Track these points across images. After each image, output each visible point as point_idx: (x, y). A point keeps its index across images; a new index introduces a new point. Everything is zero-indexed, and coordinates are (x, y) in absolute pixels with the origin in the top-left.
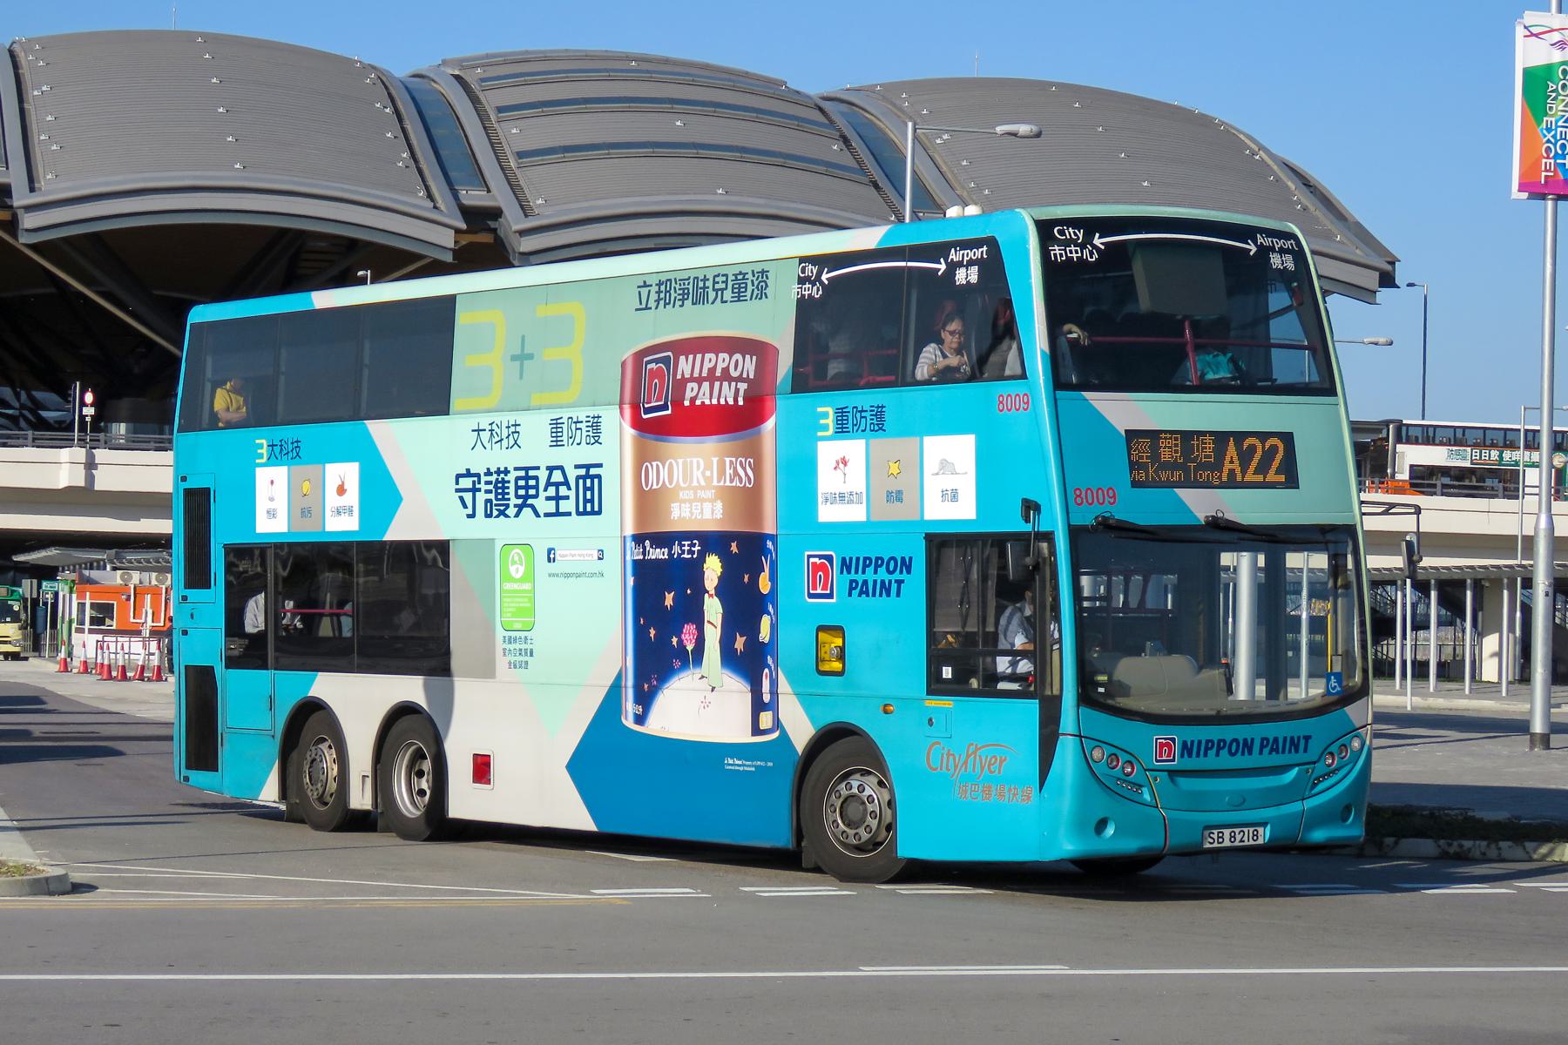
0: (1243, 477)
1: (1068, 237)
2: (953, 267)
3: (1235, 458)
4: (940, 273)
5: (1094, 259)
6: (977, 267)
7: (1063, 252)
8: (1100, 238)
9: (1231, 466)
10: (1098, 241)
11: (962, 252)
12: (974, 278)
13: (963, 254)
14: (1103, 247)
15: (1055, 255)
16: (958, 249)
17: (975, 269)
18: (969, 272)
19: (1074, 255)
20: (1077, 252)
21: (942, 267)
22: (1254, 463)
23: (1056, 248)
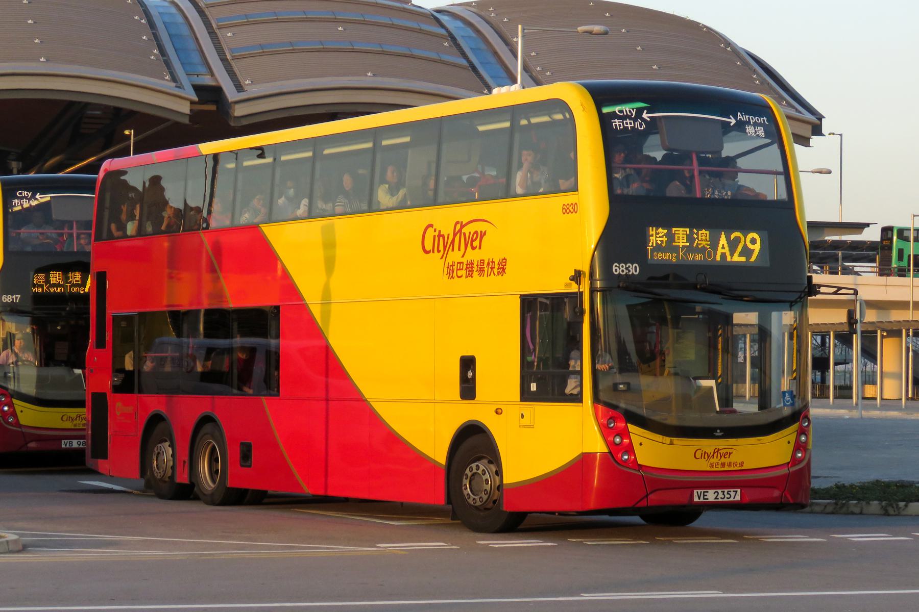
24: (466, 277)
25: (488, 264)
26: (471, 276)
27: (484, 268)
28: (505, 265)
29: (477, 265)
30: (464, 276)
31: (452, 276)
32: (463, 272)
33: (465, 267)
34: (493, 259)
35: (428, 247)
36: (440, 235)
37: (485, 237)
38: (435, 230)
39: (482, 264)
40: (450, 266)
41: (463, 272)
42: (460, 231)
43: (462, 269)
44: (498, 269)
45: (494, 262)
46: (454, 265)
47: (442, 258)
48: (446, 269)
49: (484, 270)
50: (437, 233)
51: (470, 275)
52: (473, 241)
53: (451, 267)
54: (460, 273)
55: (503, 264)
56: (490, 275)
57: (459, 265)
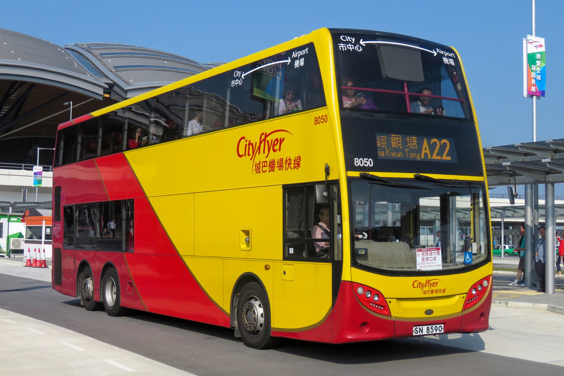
0: (431, 157)
1: (347, 40)
2: (294, 60)
3: (427, 148)
4: (288, 64)
5: (360, 51)
6: (303, 58)
7: (345, 46)
8: (363, 41)
9: (426, 152)
10: (362, 42)
11: (297, 53)
12: (302, 64)
13: (298, 53)
14: (364, 45)
15: (341, 48)
16: (296, 51)
17: (303, 59)
18: (300, 61)
19: (351, 48)
20: (352, 47)
21: (289, 61)
22: (436, 151)
23: (342, 44)
24: (269, 172)
25: (286, 161)
26: (273, 171)
27: (283, 164)
28: (300, 161)
29: (278, 163)
30: (268, 171)
31: (259, 172)
32: (267, 168)
33: (268, 164)
34: (290, 157)
35: (242, 152)
36: (250, 144)
37: (283, 142)
38: (246, 141)
39: (281, 162)
40: (258, 164)
41: (267, 168)
42: (265, 139)
43: (266, 166)
44: (294, 164)
45: (291, 160)
46: (260, 164)
47: (251, 159)
48: (254, 167)
49: (283, 166)
50: (248, 143)
51: (272, 169)
52: (274, 145)
53: (258, 165)
54: (264, 169)
55: (298, 160)
56: (287, 169)
57: (264, 163)
